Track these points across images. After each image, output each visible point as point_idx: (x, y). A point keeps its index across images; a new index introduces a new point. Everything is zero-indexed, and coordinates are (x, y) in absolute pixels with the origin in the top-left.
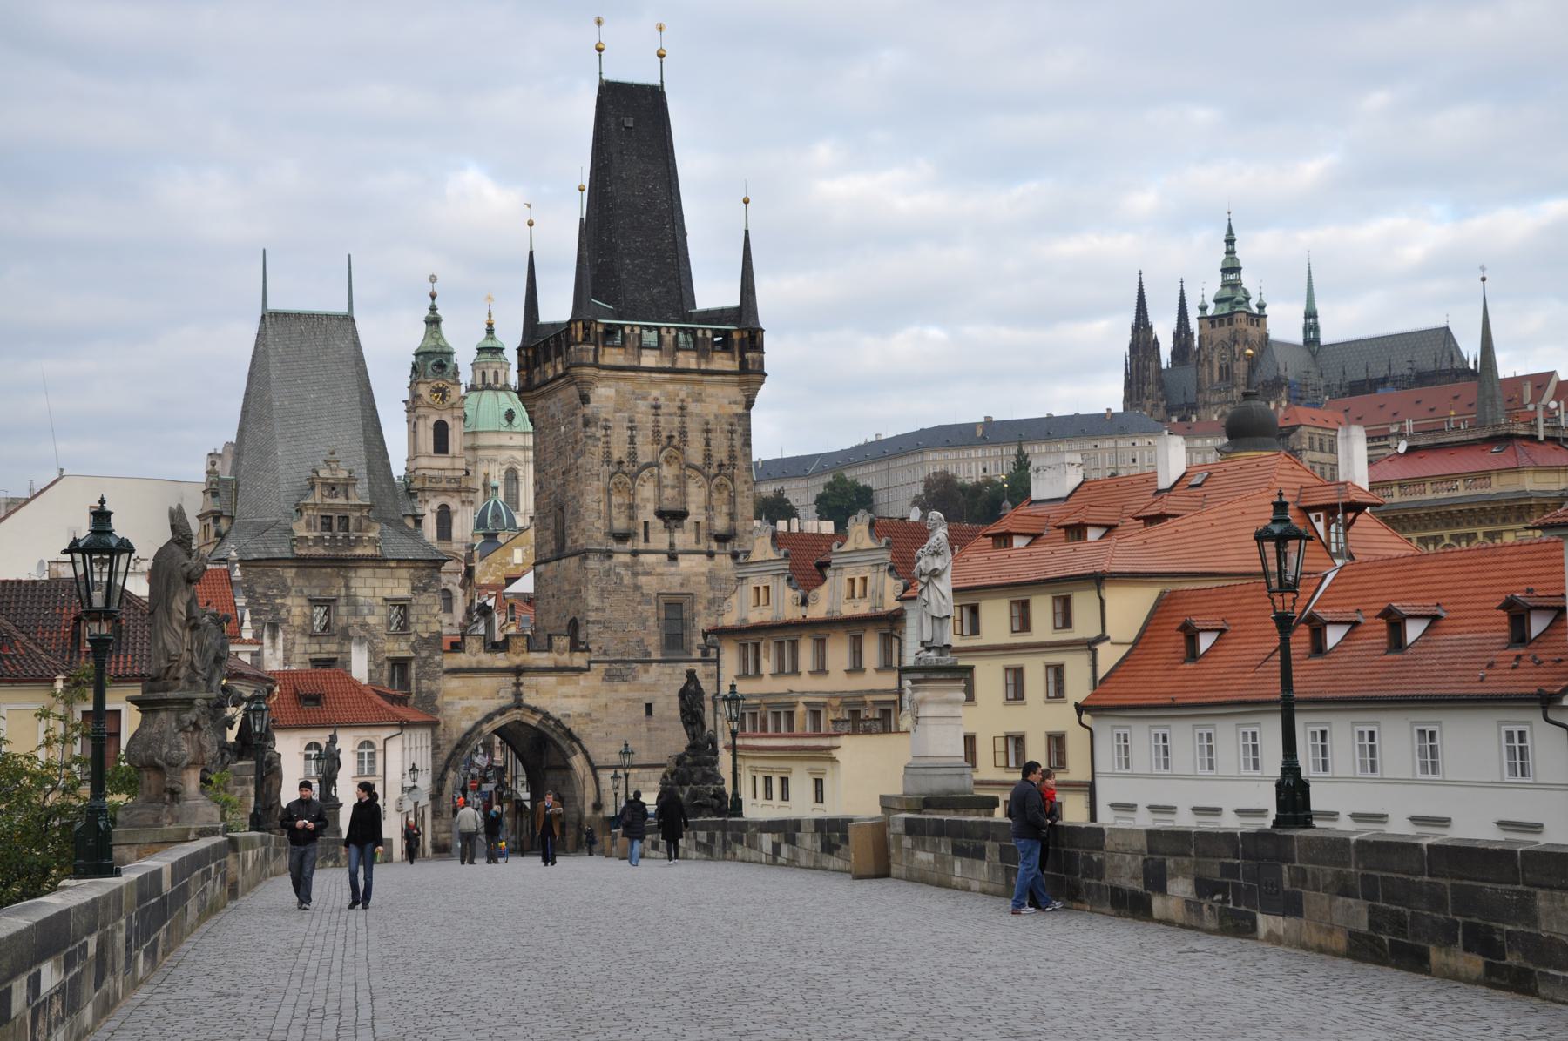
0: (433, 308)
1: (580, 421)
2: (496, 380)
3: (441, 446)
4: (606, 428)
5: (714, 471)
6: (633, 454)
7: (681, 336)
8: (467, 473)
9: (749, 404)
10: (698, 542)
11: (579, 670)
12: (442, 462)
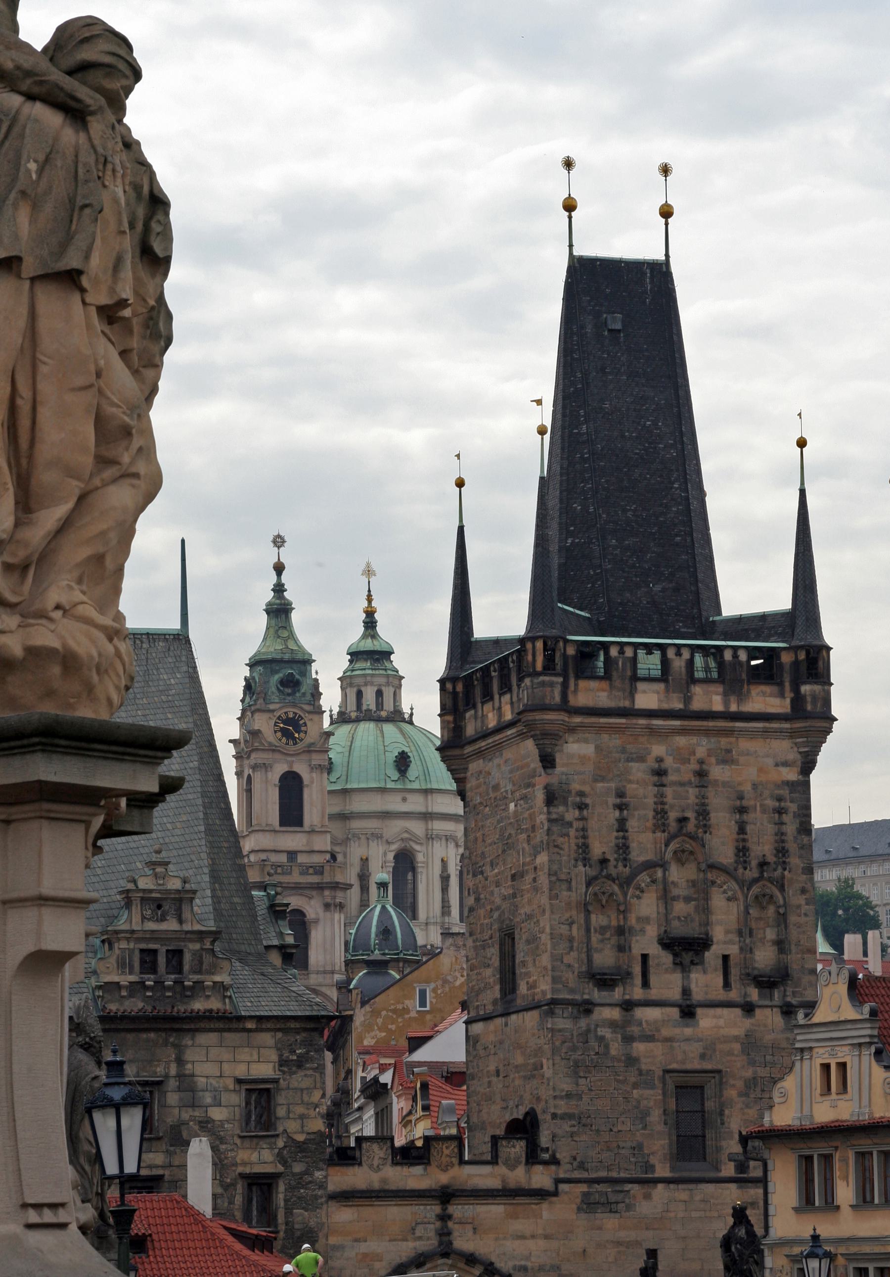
0: (279, 589)
1: (540, 796)
2: (380, 705)
3: (291, 813)
4: (582, 807)
5: (752, 873)
6: (623, 848)
7: (699, 660)
8: (334, 857)
9: (808, 766)
10: (727, 985)
11: (541, 1194)
12: (293, 840)
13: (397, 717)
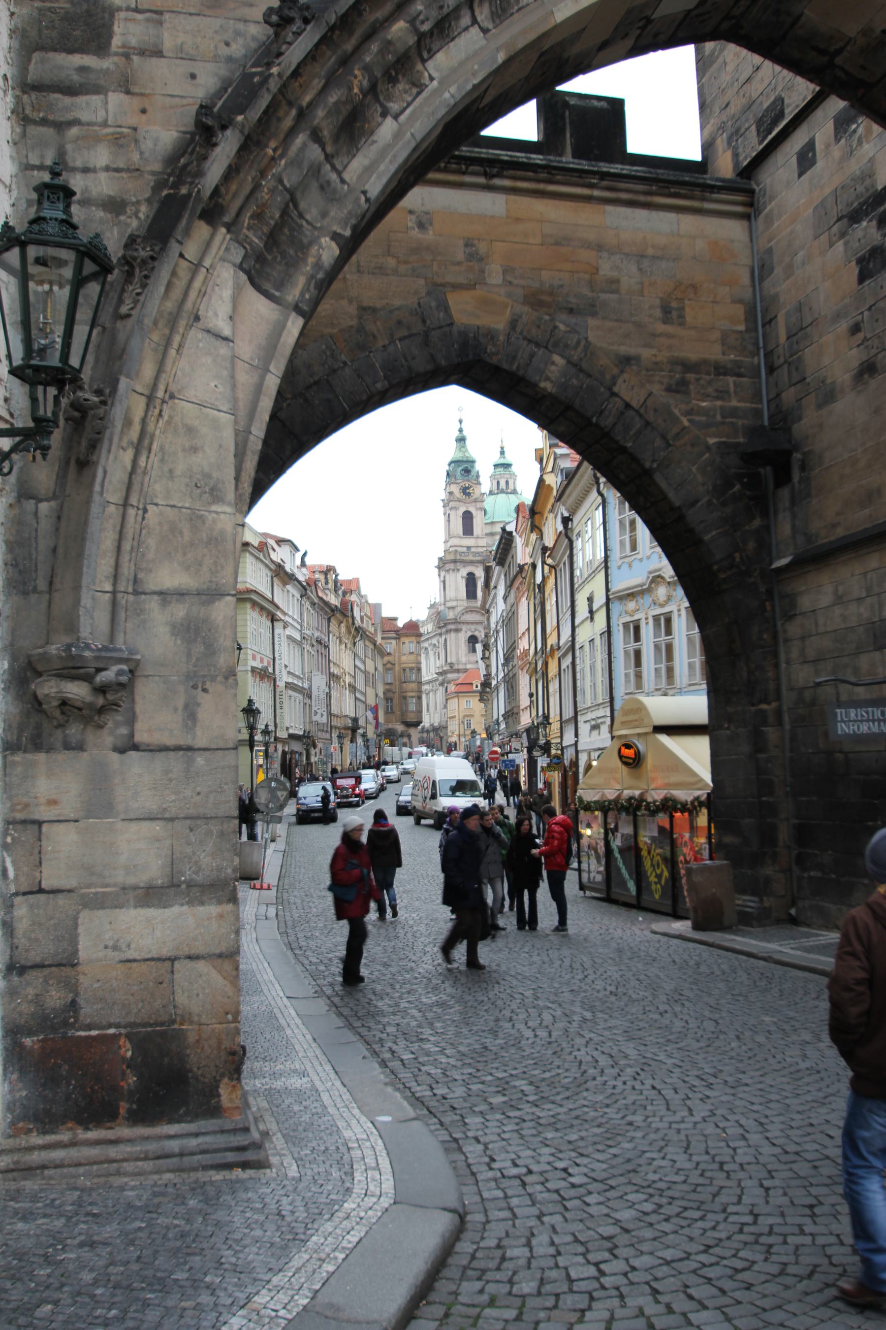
0: (461, 430)
3: (468, 529)
12: (469, 541)
13: (514, 492)
